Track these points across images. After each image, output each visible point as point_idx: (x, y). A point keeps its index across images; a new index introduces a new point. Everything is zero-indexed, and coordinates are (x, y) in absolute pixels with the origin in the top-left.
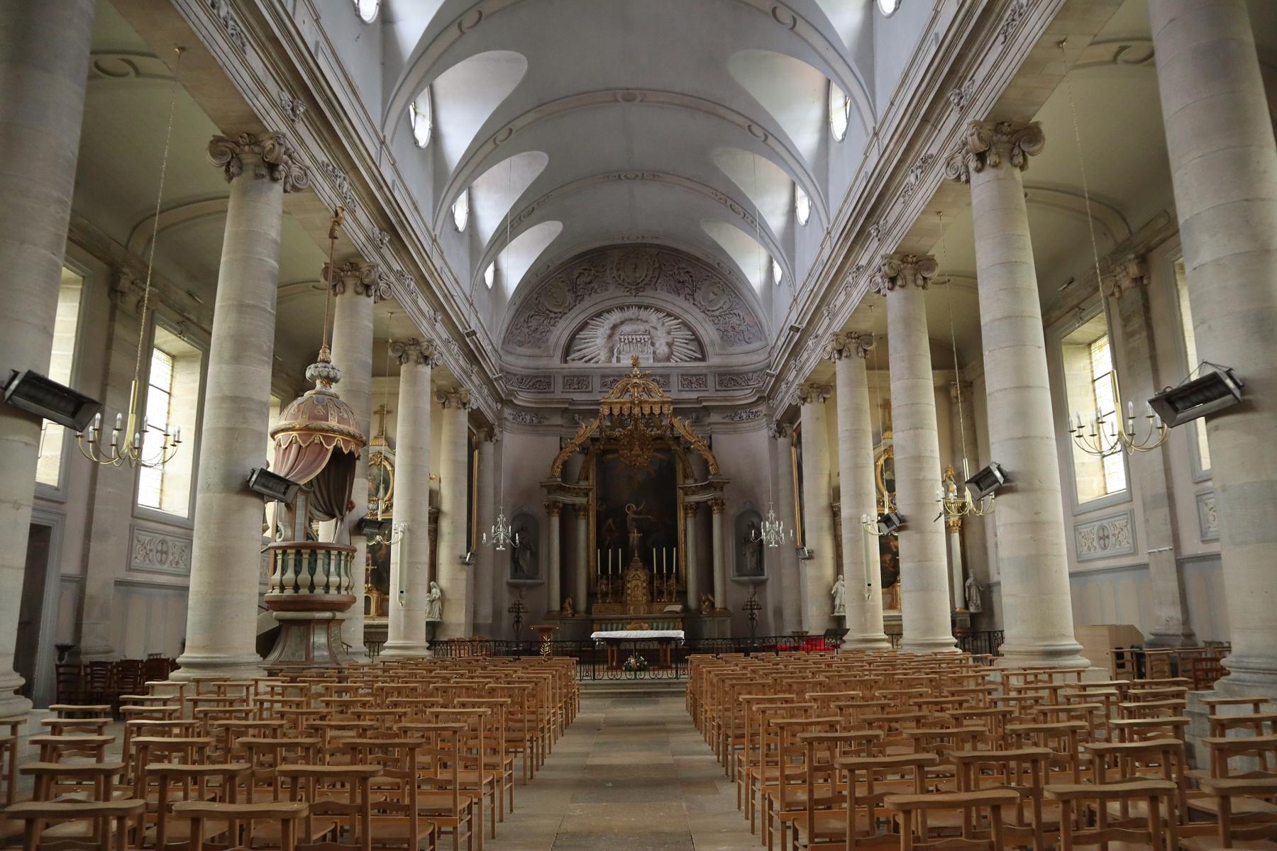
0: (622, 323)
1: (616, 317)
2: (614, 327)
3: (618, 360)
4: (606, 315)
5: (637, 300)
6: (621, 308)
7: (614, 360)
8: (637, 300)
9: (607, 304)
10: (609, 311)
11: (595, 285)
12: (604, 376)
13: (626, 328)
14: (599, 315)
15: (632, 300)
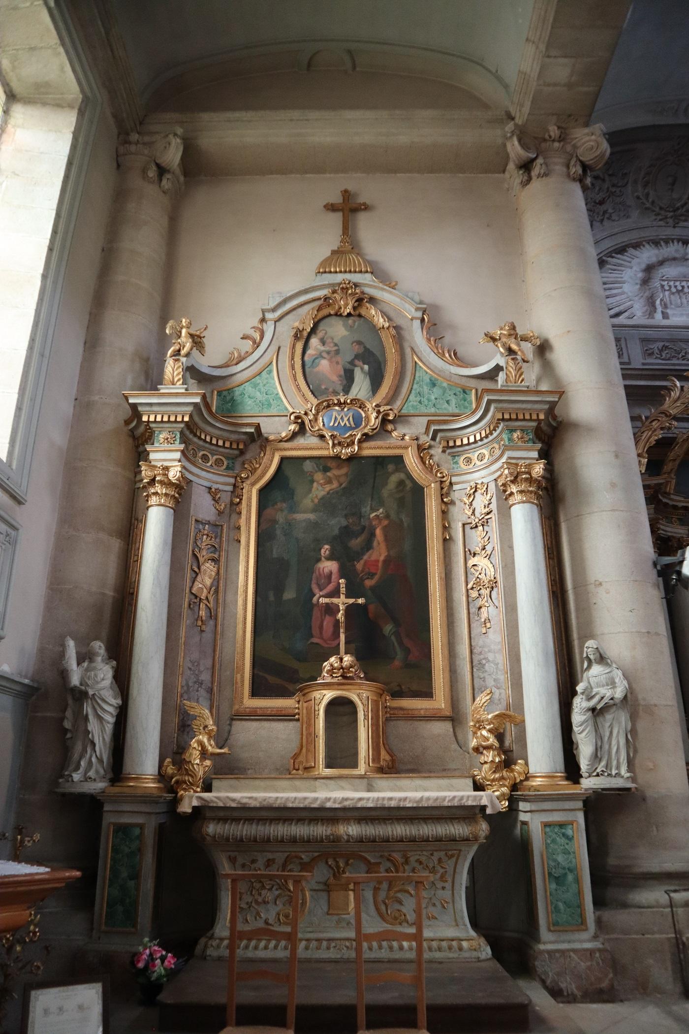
0: (661, 263)
1: (648, 255)
2: (649, 269)
3: (665, 316)
4: (631, 251)
5: (678, 232)
6: (656, 243)
7: (658, 316)
8: (678, 232)
9: (633, 236)
10: (637, 246)
11: (608, 206)
12: (645, 341)
13: (670, 271)
14: (622, 250)
15: (669, 232)
